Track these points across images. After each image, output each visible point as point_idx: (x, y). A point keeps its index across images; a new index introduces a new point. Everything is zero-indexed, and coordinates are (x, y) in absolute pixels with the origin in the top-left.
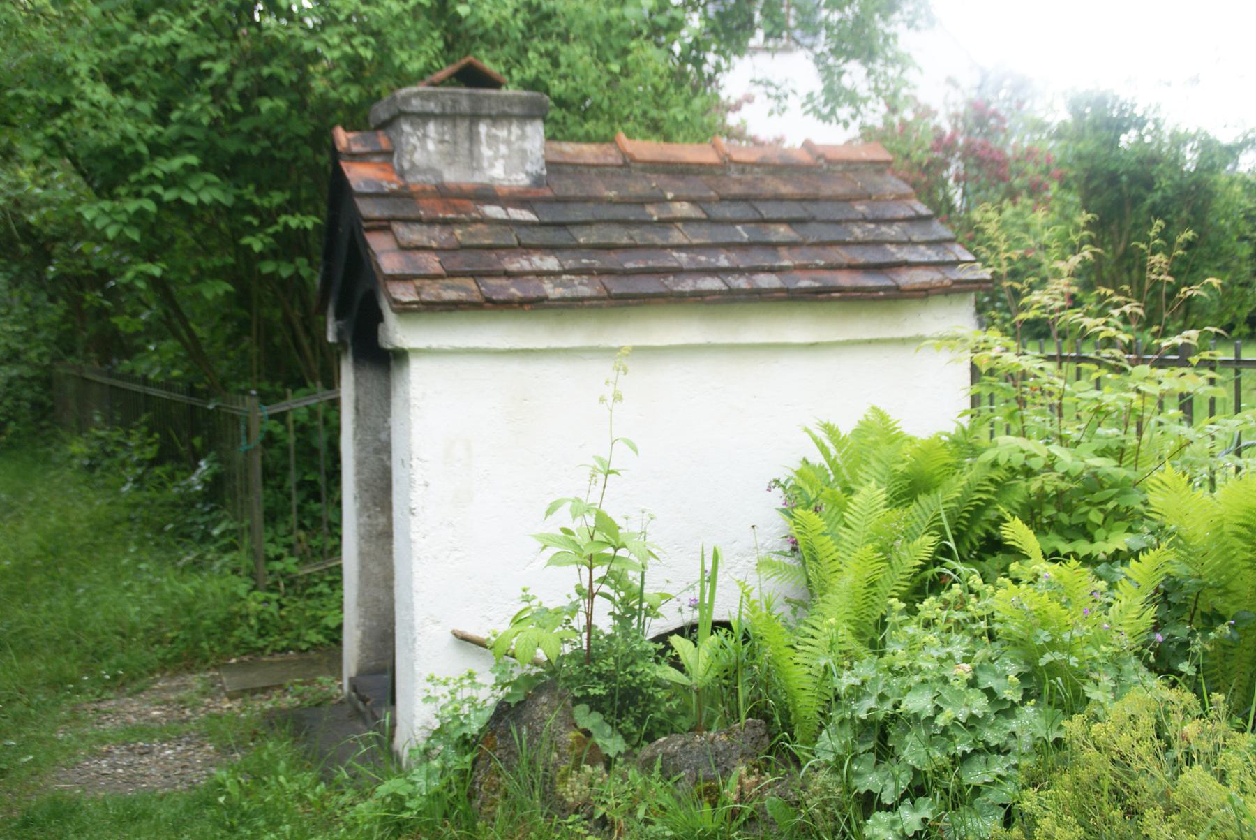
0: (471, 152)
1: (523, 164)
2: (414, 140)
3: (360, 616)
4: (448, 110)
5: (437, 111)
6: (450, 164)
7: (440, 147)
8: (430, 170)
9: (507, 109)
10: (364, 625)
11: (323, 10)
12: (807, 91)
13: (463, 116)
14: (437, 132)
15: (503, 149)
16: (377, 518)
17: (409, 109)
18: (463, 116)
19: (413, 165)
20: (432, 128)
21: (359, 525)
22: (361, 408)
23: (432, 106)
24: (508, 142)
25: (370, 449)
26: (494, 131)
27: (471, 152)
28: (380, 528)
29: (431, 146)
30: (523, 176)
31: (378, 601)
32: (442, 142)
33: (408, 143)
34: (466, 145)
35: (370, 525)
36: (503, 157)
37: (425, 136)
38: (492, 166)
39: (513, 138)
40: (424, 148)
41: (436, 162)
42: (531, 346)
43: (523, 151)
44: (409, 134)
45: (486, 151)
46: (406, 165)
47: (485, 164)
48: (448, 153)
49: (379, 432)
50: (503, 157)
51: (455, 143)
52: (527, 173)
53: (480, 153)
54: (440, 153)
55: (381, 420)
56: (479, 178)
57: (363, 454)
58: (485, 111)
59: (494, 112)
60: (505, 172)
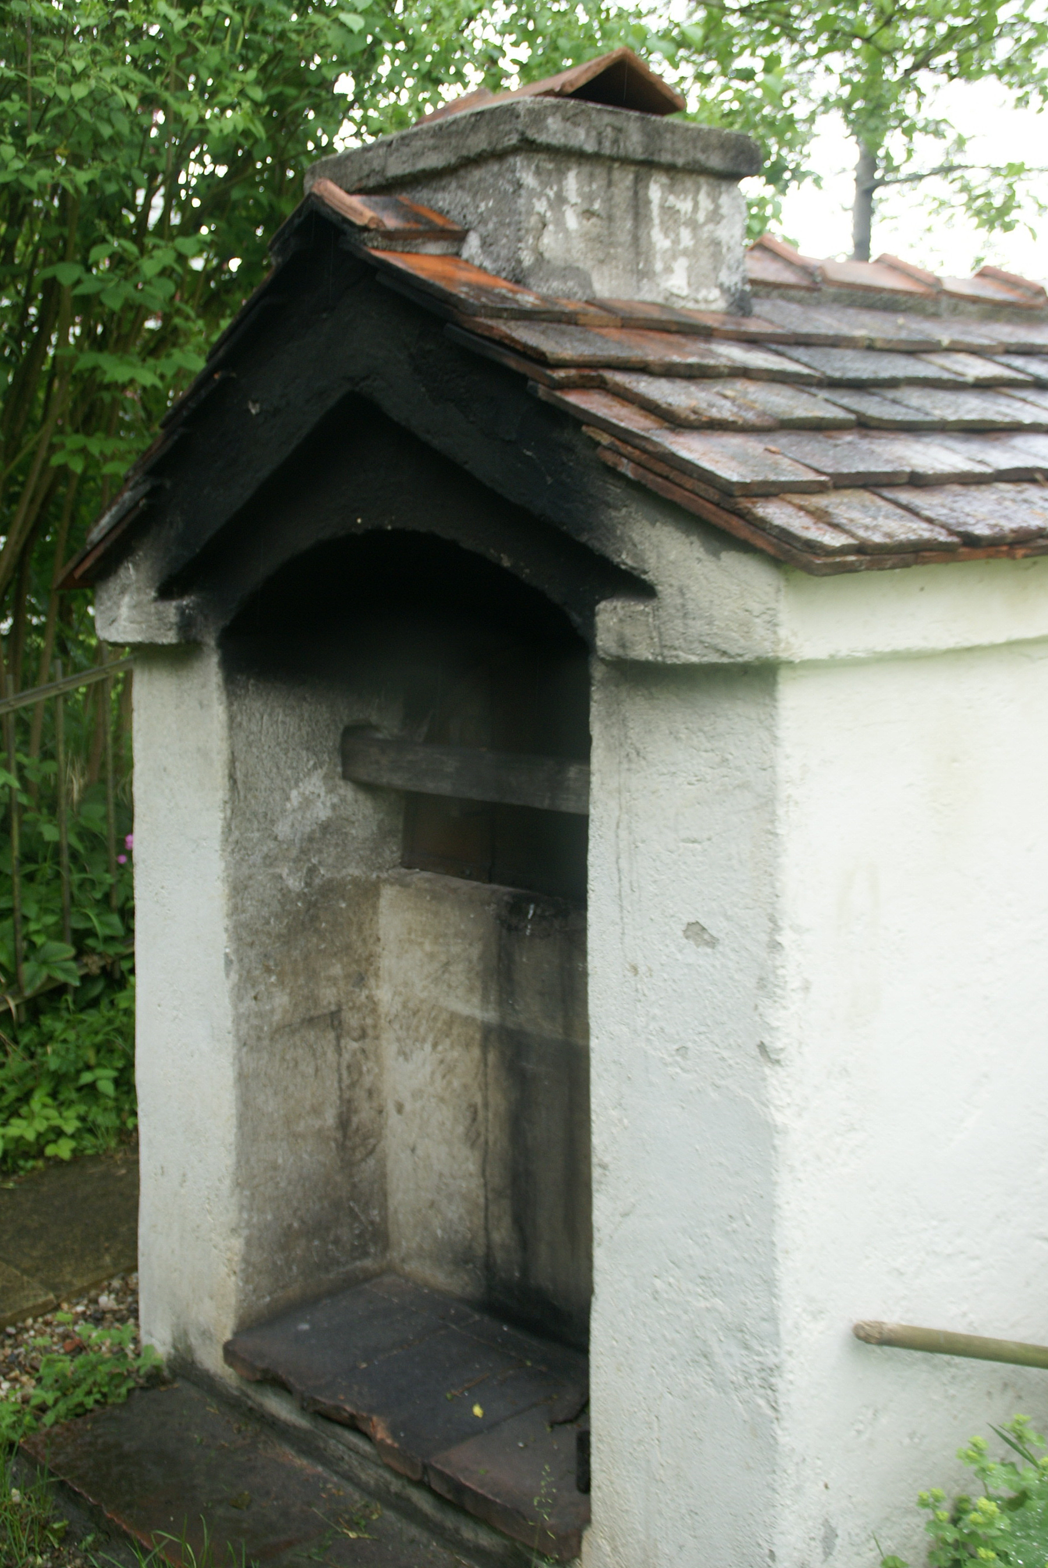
0: (636, 239)
1: (716, 269)
2: (541, 206)
3: (242, 1208)
4: (607, 149)
5: (590, 148)
6: (602, 262)
7: (588, 224)
8: (569, 271)
9: (701, 157)
10: (249, 1224)
11: (907, 46)
12: (824, 94)
13: (625, 161)
14: (580, 194)
15: (686, 237)
16: (270, 996)
17: (542, 138)
18: (625, 161)
19: (540, 257)
20: (572, 182)
21: (238, 1019)
22: (239, 775)
23: (581, 138)
24: (694, 225)
25: (257, 858)
26: (672, 199)
27: (636, 239)
28: (277, 1017)
29: (572, 221)
30: (715, 293)
31: (275, 1167)
32: (588, 214)
33: (530, 212)
34: (629, 225)
35: (260, 1015)
36: (685, 253)
37: (561, 200)
38: (669, 270)
39: (701, 217)
40: (560, 223)
41: (579, 253)
42: (984, 639)
43: (716, 243)
44: (532, 194)
45: (660, 240)
46: (527, 259)
47: (659, 266)
48: (598, 239)
49: (273, 822)
50: (685, 253)
51: (610, 218)
52: (721, 286)
53: (650, 244)
54: (585, 236)
55: (277, 796)
56: (648, 294)
57: (245, 870)
58: (666, 158)
59: (680, 161)
60: (689, 284)
